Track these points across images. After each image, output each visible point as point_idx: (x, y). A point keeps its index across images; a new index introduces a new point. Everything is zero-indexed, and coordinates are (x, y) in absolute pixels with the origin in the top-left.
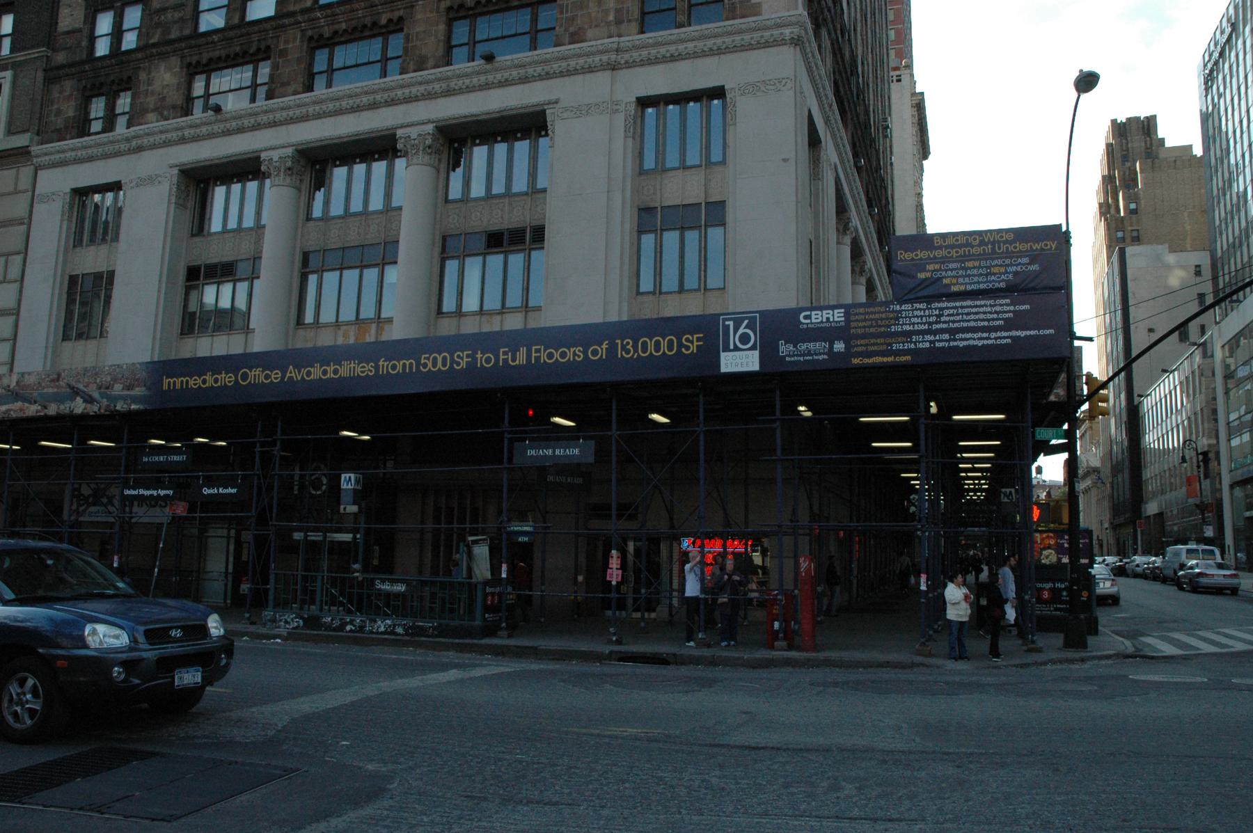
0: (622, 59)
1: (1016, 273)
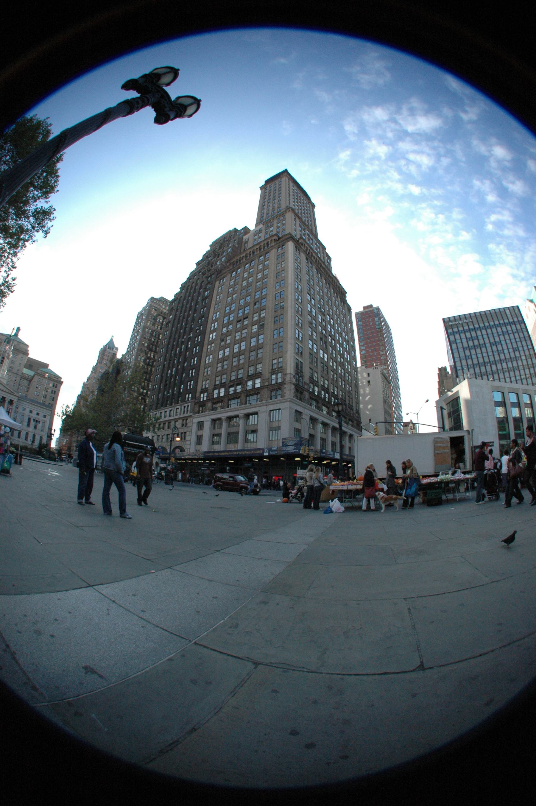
0: (268, 404)
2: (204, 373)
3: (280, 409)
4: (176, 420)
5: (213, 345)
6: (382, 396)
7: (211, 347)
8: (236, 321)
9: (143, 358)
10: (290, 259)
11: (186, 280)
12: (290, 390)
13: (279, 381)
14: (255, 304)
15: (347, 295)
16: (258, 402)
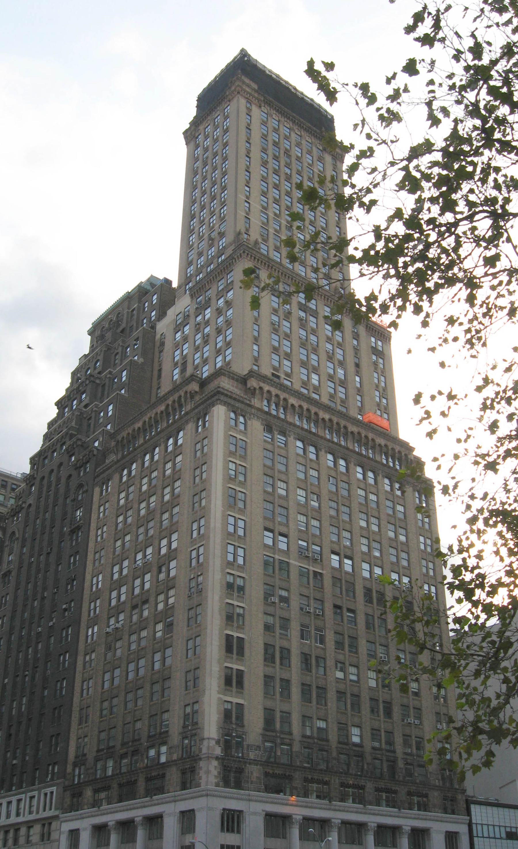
4: (29, 825)
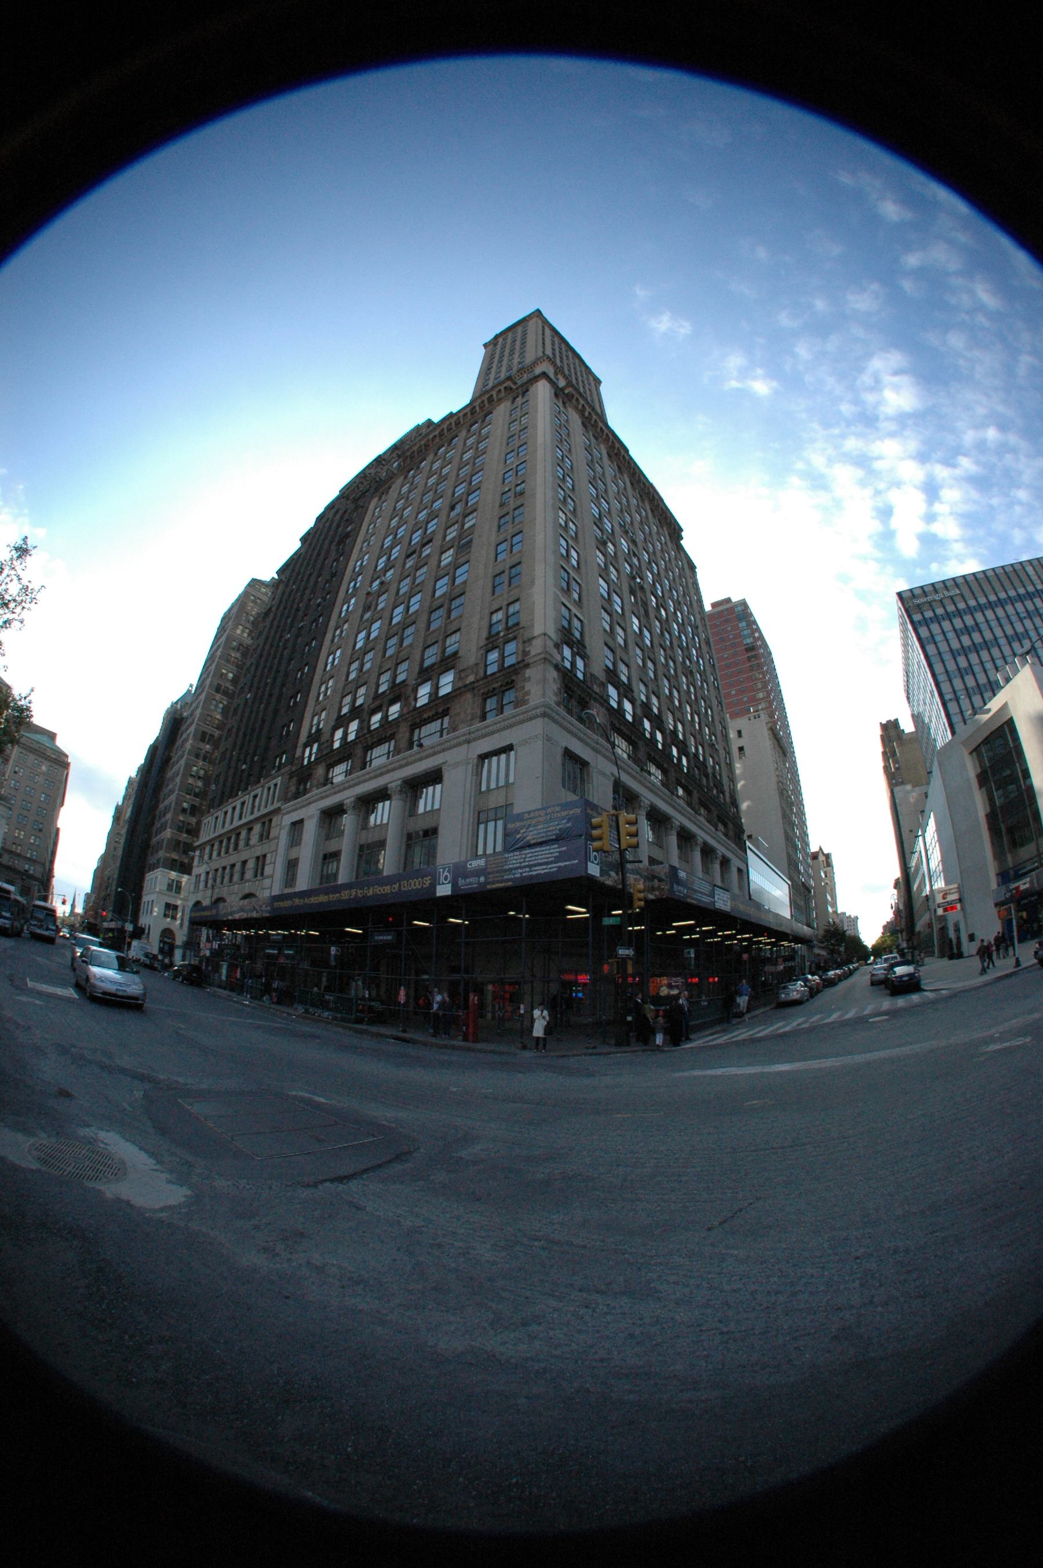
1: (560, 830)
2: (319, 694)
3: (510, 748)
5: (346, 626)
6: (774, 780)
7: (342, 632)
8: (403, 556)
9: (221, 705)
10: (540, 405)
11: (312, 524)
12: (545, 680)
13: (509, 661)
14: (453, 508)
15: (683, 534)
16: (445, 737)
